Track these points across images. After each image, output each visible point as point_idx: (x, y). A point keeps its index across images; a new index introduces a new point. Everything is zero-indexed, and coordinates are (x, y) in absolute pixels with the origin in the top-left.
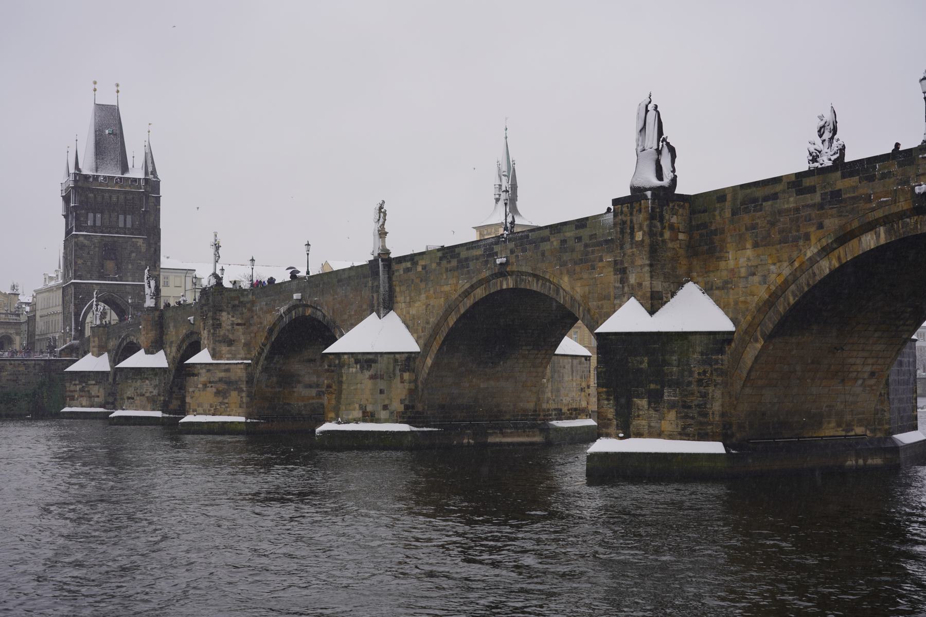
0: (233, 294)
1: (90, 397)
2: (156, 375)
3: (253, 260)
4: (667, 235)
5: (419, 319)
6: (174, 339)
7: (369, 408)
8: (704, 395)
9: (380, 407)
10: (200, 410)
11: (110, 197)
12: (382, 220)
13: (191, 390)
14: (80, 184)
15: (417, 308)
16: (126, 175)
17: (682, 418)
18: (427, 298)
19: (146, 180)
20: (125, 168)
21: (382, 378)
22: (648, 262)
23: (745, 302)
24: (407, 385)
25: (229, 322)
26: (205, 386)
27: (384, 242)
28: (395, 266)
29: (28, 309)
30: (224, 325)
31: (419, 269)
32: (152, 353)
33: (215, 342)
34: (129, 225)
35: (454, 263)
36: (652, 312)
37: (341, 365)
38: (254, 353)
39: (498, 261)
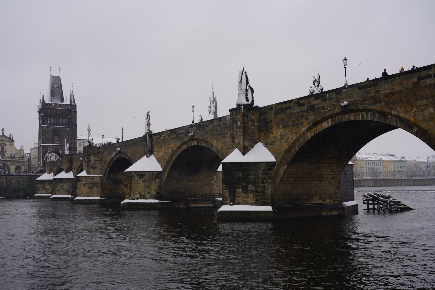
0: (95, 149)
1: (46, 190)
2: (69, 181)
3: (103, 135)
4: (250, 123)
5: (162, 158)
6: (76, 167)
7: (143, 194)
8: (264, 187)
9: (147, 193)
10: (82, 195)
11: (57, 112)
12: (148, 119)
13: (79, 187)
14: (44, 107)
15: (161, 154)
16: (63, 103)
17: (256, 196)
18: (165, 149)
19: (71, 105)
20: (63, 100)
21: (147, 181)
22: (242, 134)
23: (280, 150)
24: (157, 184)
25: (94, 160)
26: (84, 185)
27: (149, 127)
28: (154, 137)
29: (28, 155)
30: (92, 161)
31: (162, 138)
32: (68, 172)
33: (88, 167)
34: (64, 122)
35: (175, 135)
36: (244, 154)
37: (132, 177)
38: (104, 172)
39: (190, 135)
